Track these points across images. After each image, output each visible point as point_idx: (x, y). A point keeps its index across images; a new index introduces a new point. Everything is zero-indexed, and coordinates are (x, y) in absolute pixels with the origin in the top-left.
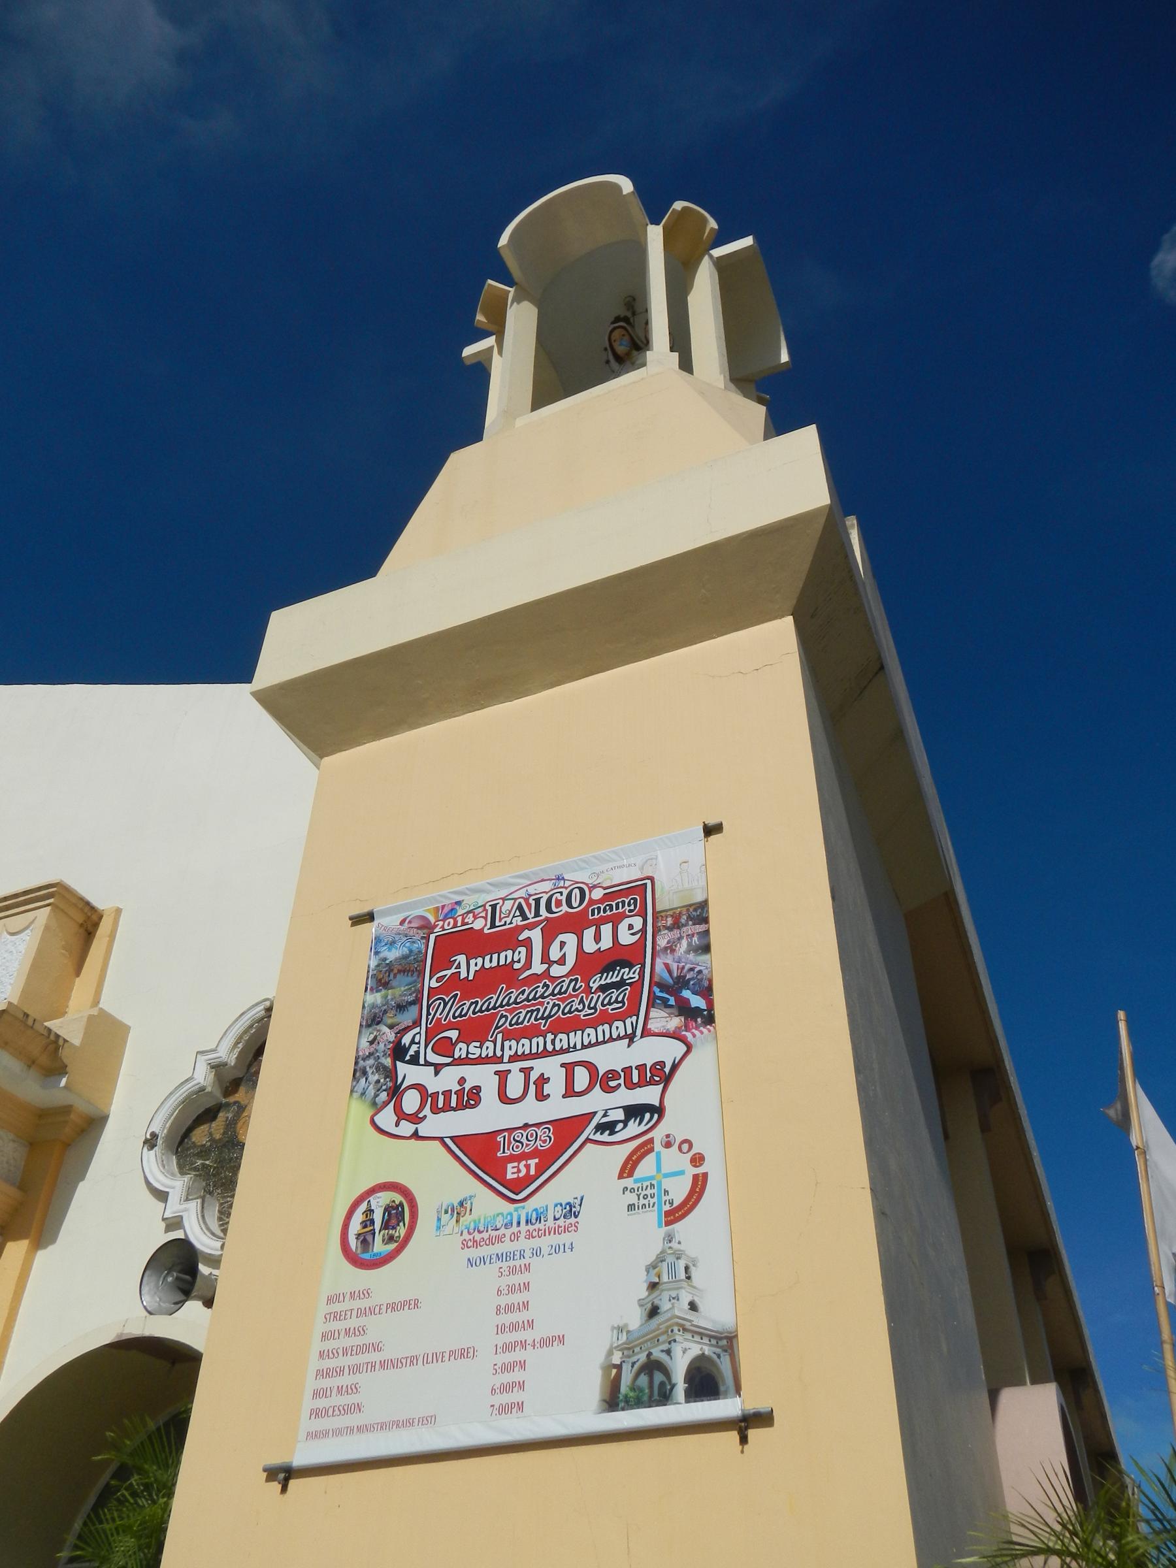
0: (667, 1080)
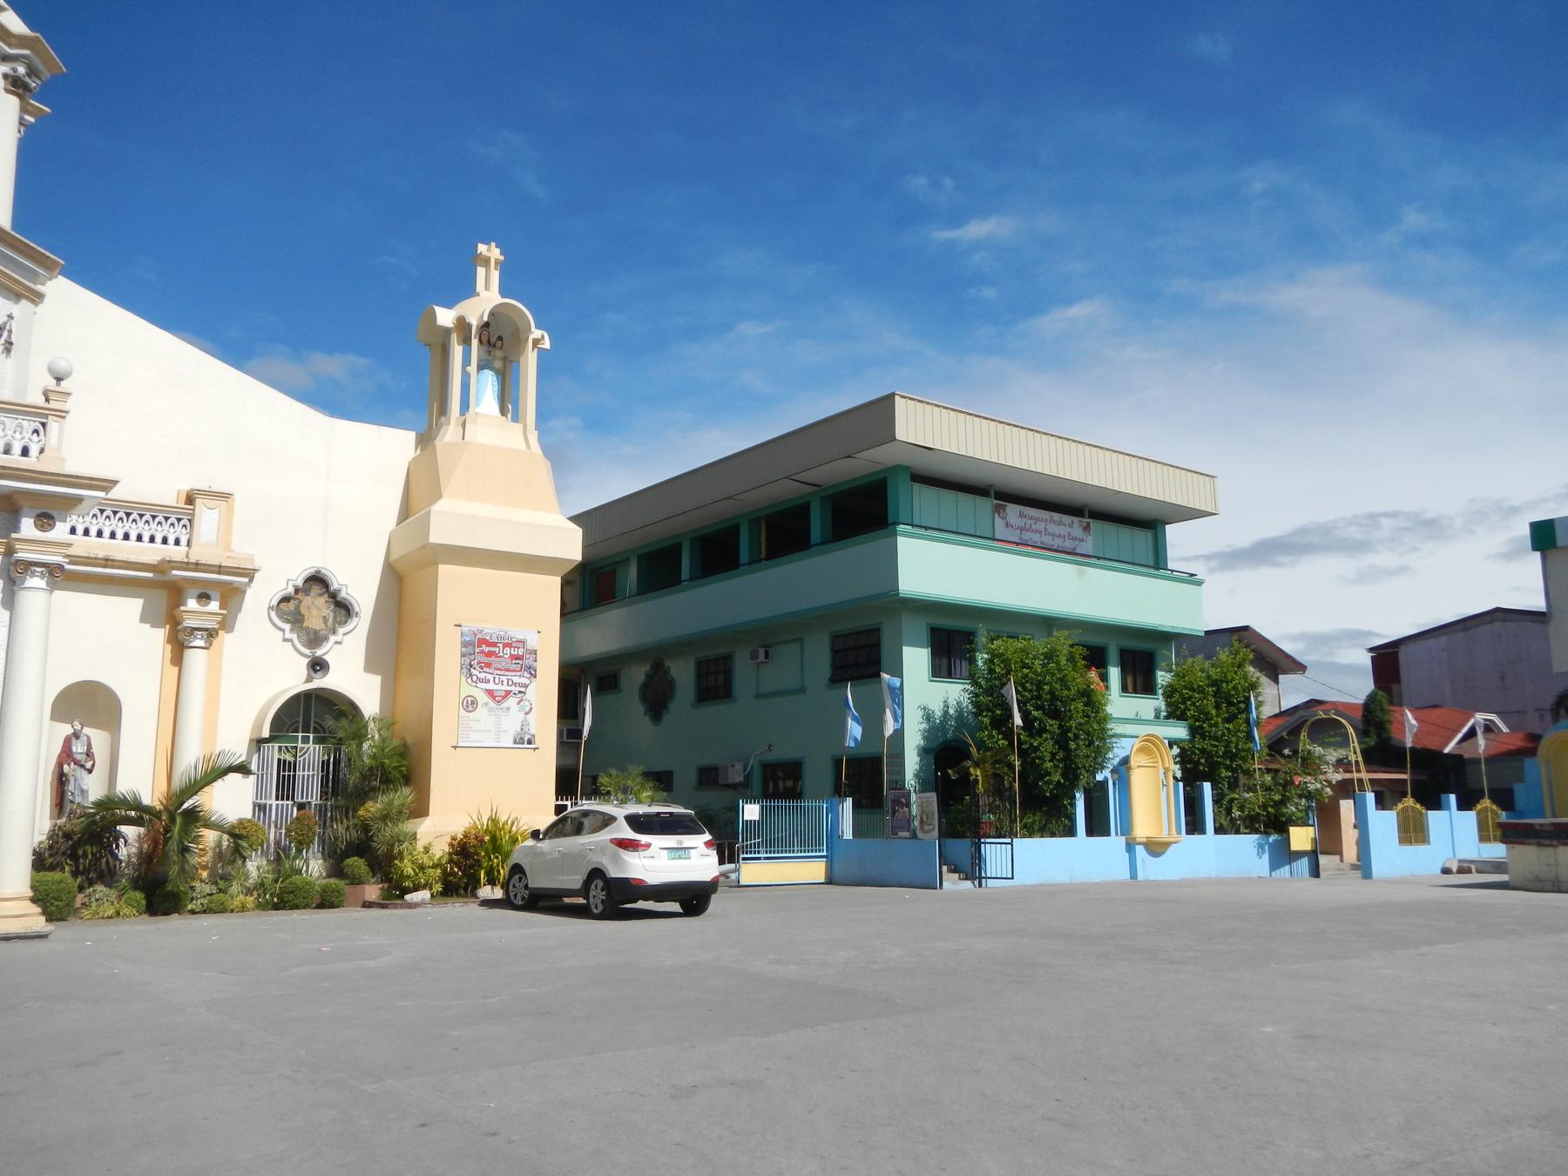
0: (527, 687)
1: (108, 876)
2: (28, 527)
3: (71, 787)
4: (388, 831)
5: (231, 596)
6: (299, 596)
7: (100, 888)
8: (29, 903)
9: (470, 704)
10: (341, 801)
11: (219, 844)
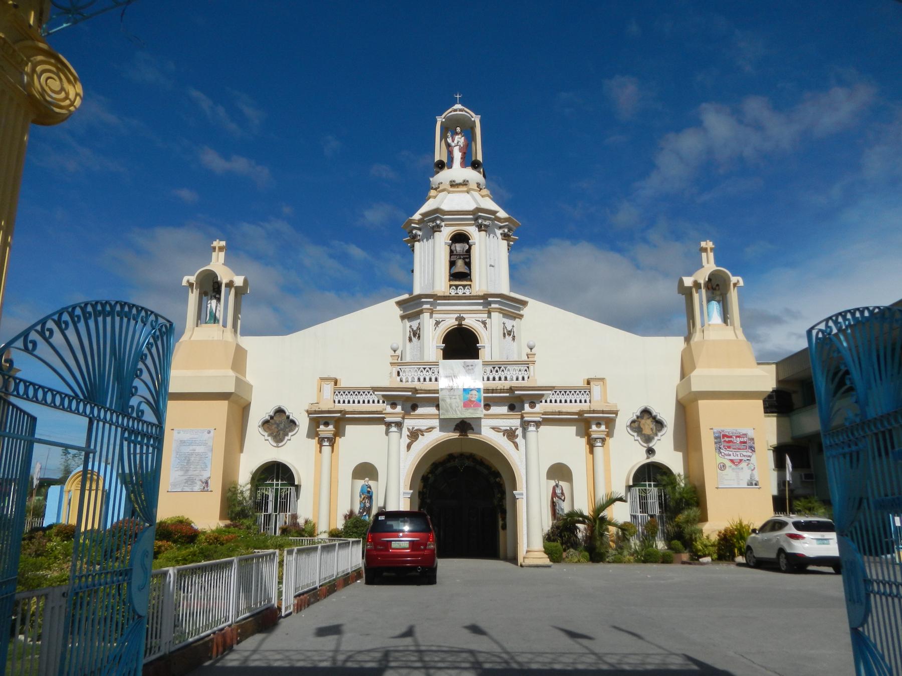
1: (575, 545)
2: (527, 406)
3: (557, 507)
4: (688, 529)
5: (610, 423)
6: (639, 420)
7: (572, 551)
8: (543, 553)
9: (723, 467)
10: (669, 514)
11: (617, 533)
